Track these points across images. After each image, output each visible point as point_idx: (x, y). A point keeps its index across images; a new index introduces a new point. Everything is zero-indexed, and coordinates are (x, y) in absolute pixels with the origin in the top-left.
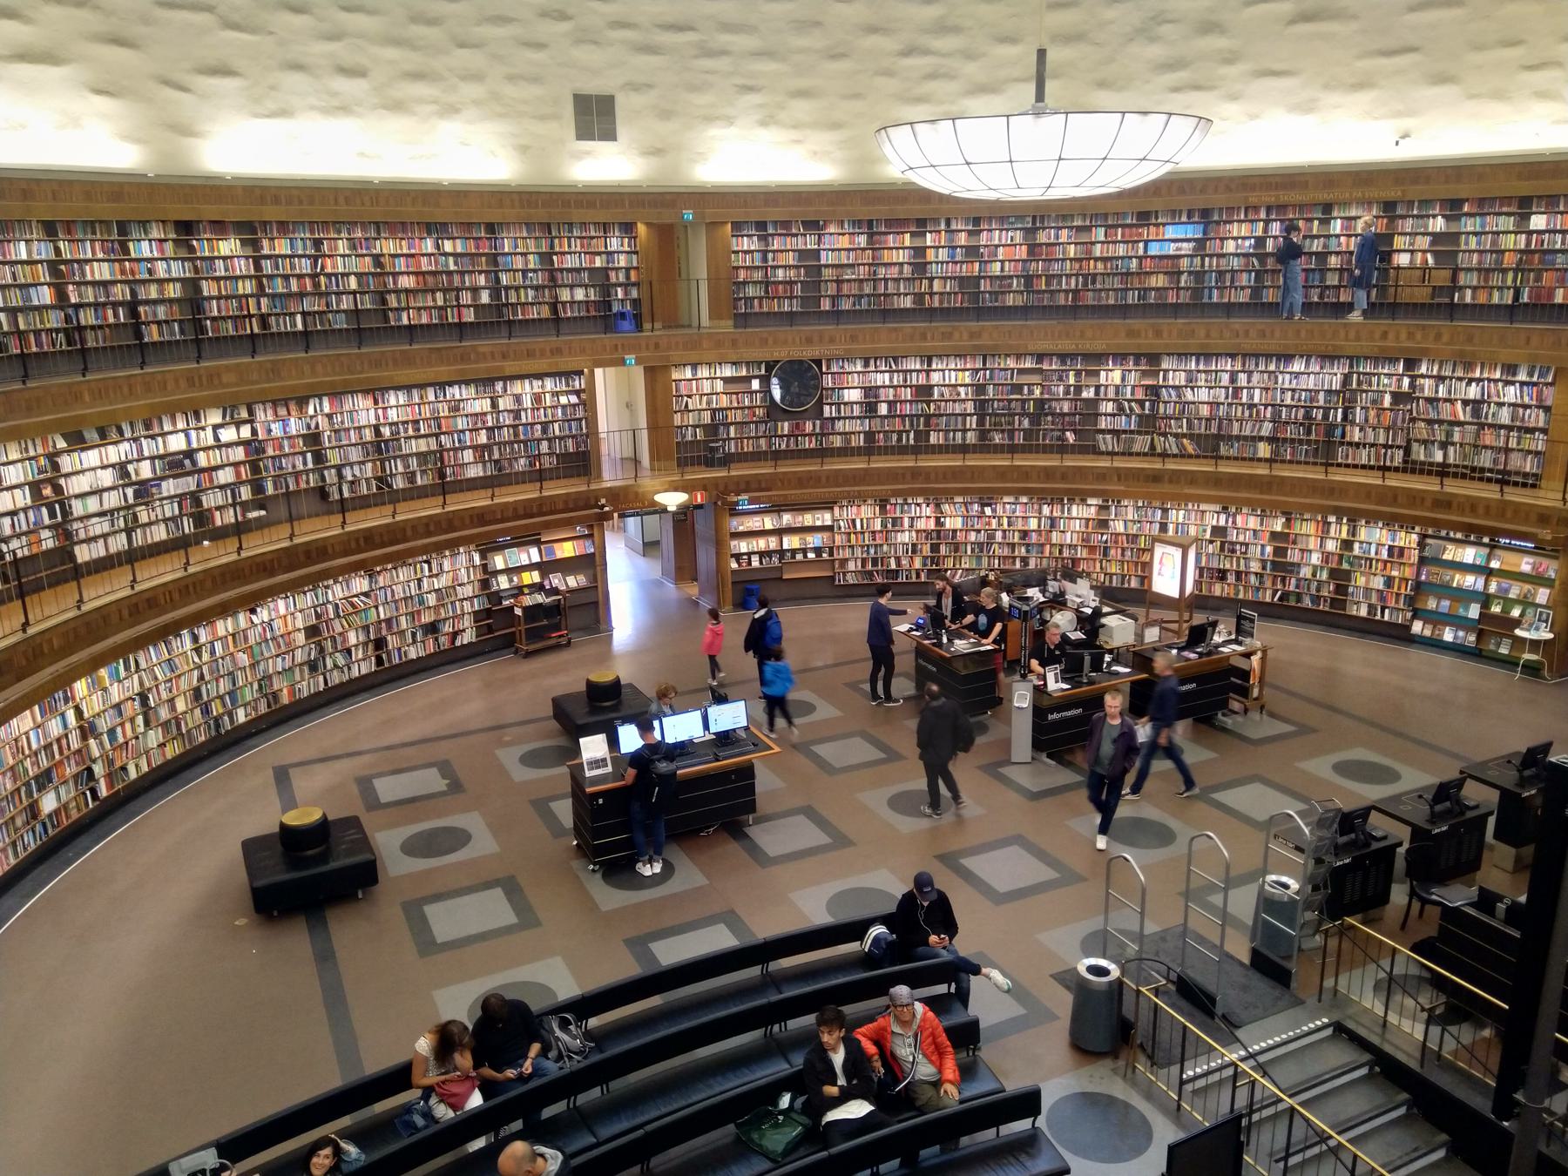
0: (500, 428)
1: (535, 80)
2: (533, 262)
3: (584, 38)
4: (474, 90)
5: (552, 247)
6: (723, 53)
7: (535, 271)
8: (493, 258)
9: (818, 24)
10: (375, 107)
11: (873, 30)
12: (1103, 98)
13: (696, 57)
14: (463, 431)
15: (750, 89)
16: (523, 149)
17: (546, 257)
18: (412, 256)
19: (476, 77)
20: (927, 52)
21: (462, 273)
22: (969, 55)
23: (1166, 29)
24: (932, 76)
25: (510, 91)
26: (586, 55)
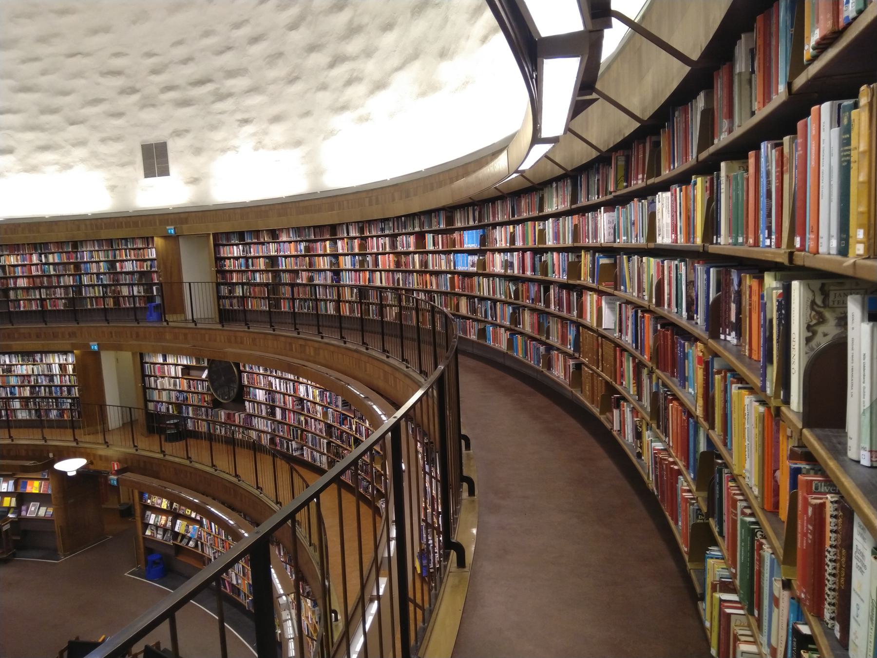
0: (40, 387)
1: (118, 139)
2: (103, 267)
3: (148, 103)
4: (80, 152)
5: (115, 256)
6: (230, 95)
7: (104, 274)
8: (77, 266)
10: (19, 171)
13: (213, 102)
14: (14, 387)
15: (246, 121)
16: (113, 188)
17: (112, 264)
18: (24, 265)
19: (81, 143)
21: (58, 276)
25: (103, 149)
26: (149, 115)
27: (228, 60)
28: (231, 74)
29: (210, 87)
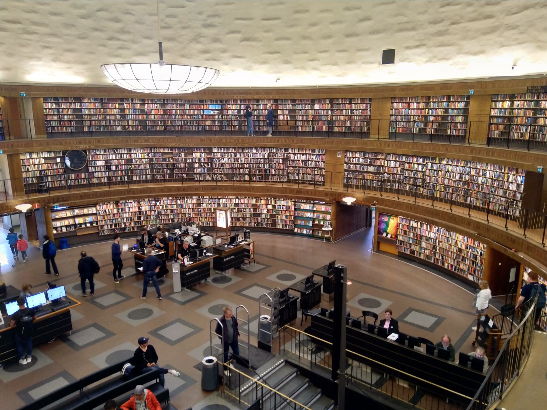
6: (34, 33)
9: (74, 26)
11: (96, 30)
12: (183, 61)
13: (22, 34)
15: (48, 47)
20: (118, 39)
22: (135, 42)
23: (202, 39)
24: (121, 48)
27: (34, 17)
28: (35, 23)
29: (19, 26)
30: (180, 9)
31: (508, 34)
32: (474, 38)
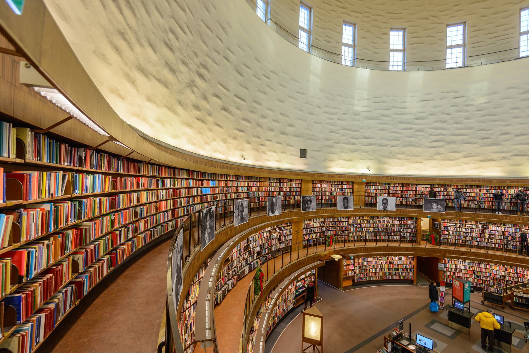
30: (182, 32)
31: (363, 154)
32: (346, 153)
